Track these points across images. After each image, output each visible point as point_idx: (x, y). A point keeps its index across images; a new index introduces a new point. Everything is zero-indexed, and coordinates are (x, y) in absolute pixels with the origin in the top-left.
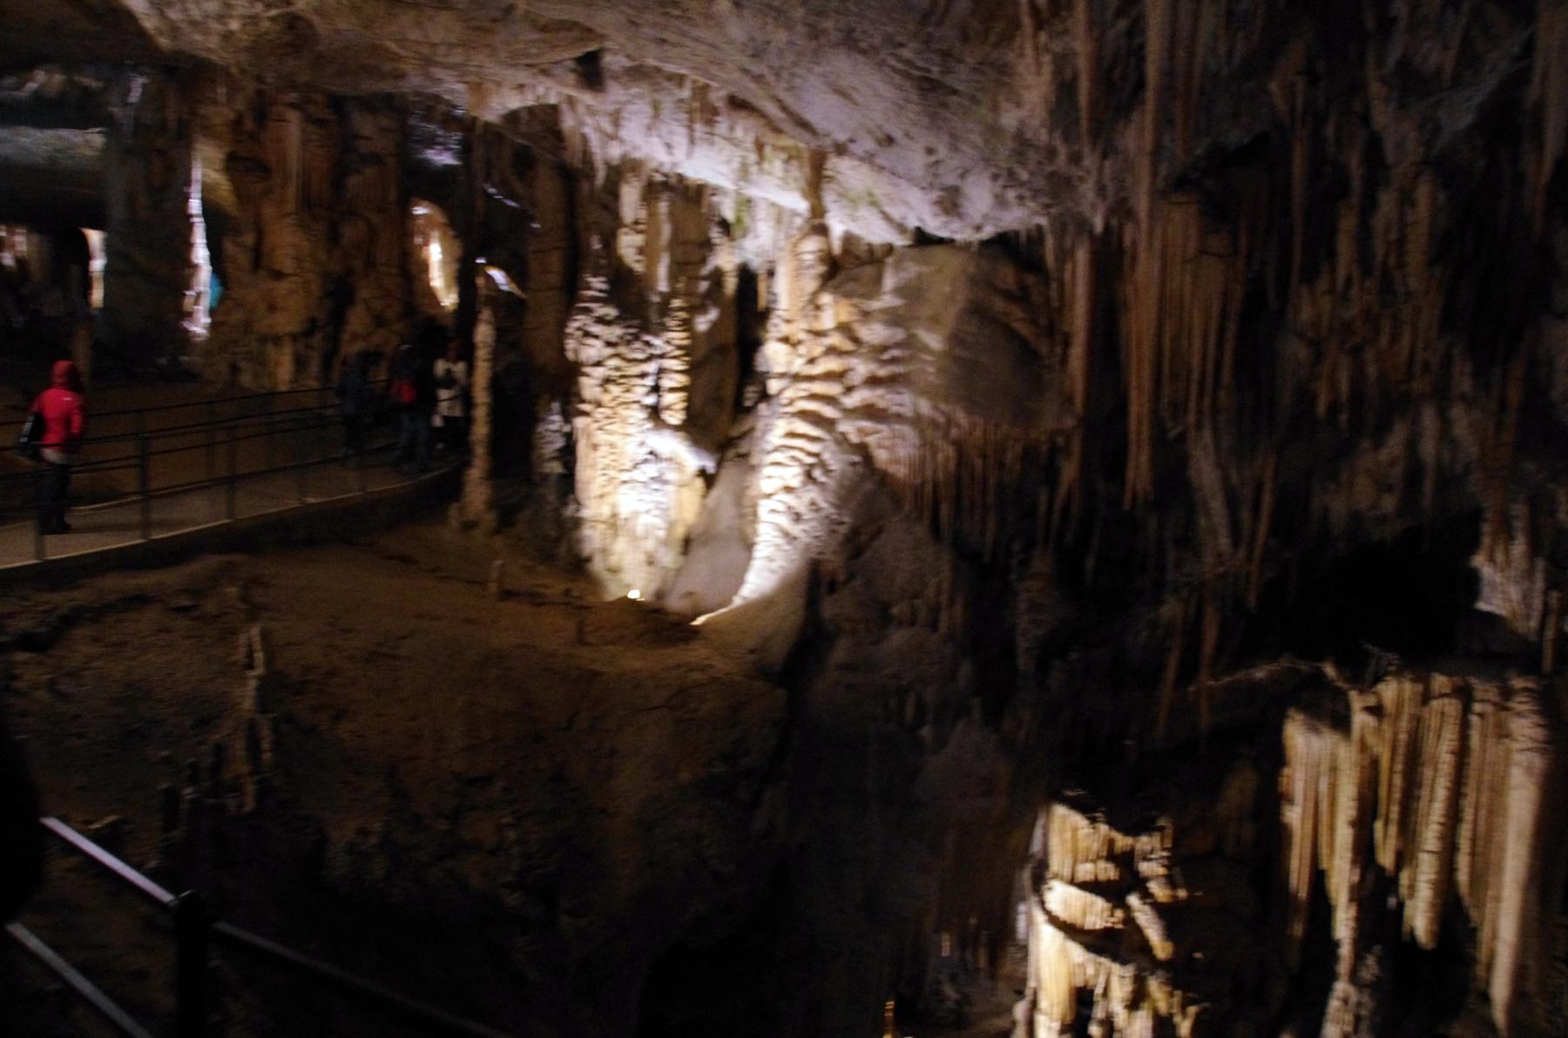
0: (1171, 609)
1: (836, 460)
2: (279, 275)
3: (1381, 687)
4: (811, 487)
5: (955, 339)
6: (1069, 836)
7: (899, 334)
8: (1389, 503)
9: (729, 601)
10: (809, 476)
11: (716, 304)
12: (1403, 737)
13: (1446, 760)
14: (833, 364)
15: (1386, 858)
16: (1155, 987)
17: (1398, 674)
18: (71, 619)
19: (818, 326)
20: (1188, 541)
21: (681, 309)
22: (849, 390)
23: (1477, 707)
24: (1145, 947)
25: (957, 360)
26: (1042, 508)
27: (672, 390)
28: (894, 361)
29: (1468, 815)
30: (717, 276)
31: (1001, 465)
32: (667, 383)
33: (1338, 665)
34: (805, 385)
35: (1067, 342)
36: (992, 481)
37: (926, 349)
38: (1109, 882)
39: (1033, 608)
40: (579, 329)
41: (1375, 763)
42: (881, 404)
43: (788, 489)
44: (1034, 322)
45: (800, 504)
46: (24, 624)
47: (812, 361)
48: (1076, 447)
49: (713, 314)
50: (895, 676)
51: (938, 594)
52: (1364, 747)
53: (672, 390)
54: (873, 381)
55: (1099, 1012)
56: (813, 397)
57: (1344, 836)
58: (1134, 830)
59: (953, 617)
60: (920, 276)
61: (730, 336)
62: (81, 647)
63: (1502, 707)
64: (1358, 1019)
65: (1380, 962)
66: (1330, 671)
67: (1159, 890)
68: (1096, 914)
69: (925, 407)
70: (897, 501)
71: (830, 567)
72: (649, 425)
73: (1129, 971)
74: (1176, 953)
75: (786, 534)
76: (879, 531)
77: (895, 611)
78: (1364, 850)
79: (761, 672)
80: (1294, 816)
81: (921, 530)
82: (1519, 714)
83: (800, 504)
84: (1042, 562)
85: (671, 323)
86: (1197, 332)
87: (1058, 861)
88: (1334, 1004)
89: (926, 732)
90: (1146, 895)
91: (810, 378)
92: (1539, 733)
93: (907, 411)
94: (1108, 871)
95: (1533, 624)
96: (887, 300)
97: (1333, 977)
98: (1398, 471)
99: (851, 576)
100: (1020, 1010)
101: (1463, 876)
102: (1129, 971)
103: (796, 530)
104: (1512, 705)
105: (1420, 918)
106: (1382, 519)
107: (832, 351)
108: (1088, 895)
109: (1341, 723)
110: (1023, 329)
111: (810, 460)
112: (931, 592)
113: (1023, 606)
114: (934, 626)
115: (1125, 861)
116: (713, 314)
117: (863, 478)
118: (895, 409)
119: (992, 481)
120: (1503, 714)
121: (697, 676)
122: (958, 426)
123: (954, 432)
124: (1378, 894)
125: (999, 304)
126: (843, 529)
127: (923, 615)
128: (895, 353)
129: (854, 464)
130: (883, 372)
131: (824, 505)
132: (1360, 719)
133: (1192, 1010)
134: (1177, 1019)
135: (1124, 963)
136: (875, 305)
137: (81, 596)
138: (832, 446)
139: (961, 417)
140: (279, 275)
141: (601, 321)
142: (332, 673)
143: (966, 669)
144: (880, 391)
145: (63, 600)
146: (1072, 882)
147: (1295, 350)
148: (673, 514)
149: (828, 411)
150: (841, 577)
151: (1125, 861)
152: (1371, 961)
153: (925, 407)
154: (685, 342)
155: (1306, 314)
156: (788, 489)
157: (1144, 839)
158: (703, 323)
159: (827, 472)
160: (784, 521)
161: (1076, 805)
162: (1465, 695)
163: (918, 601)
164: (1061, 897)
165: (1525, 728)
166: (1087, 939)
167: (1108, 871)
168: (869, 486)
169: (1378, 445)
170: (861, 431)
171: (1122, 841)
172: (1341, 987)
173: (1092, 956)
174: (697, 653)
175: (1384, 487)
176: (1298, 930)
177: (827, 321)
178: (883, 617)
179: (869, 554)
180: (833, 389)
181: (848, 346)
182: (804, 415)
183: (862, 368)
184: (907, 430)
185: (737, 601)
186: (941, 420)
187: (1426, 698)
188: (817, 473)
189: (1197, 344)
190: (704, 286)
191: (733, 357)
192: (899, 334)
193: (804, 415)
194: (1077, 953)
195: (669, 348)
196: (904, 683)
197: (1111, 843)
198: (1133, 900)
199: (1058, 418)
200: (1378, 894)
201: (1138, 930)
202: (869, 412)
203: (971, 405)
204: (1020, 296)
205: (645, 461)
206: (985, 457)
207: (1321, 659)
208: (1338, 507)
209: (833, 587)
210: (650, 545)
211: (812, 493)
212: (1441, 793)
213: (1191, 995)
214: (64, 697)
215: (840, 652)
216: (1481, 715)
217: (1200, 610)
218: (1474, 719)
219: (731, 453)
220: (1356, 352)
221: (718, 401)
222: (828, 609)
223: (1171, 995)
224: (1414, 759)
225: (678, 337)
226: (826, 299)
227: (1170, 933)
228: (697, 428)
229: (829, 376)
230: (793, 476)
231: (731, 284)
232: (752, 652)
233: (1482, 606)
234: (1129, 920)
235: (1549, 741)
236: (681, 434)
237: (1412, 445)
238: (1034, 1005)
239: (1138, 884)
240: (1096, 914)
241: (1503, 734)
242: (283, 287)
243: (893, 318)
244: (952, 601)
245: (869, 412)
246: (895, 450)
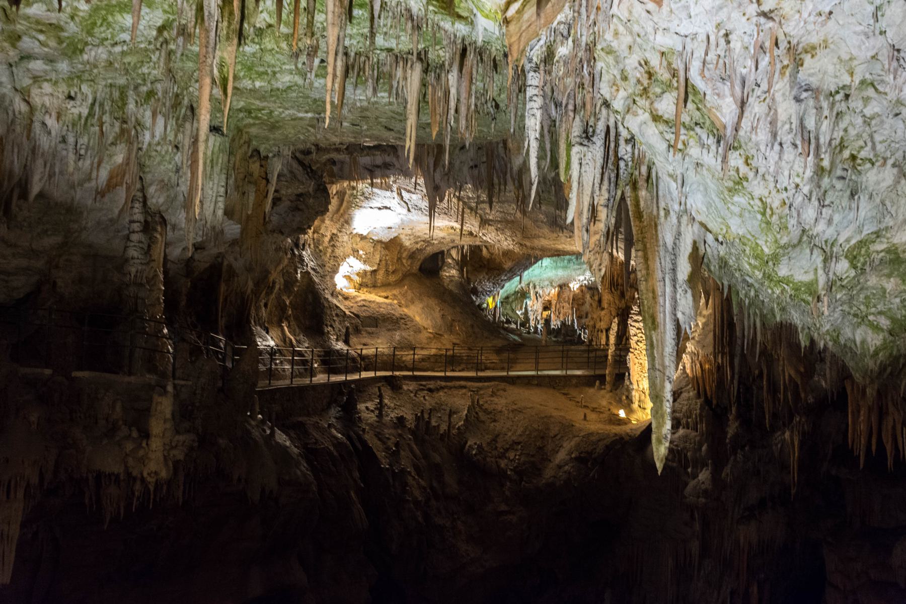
2: (603, 309)
18: (442, 388)
46: (431, 386)
62: (441, 393)
89: (689, 470)
137: (449, 384)
140: (603, 309)
141: (636, 321)
142: (501, 412)
143: (704, 448)
145: (443, 384)
214: (425, 400)
242: (603, 313)
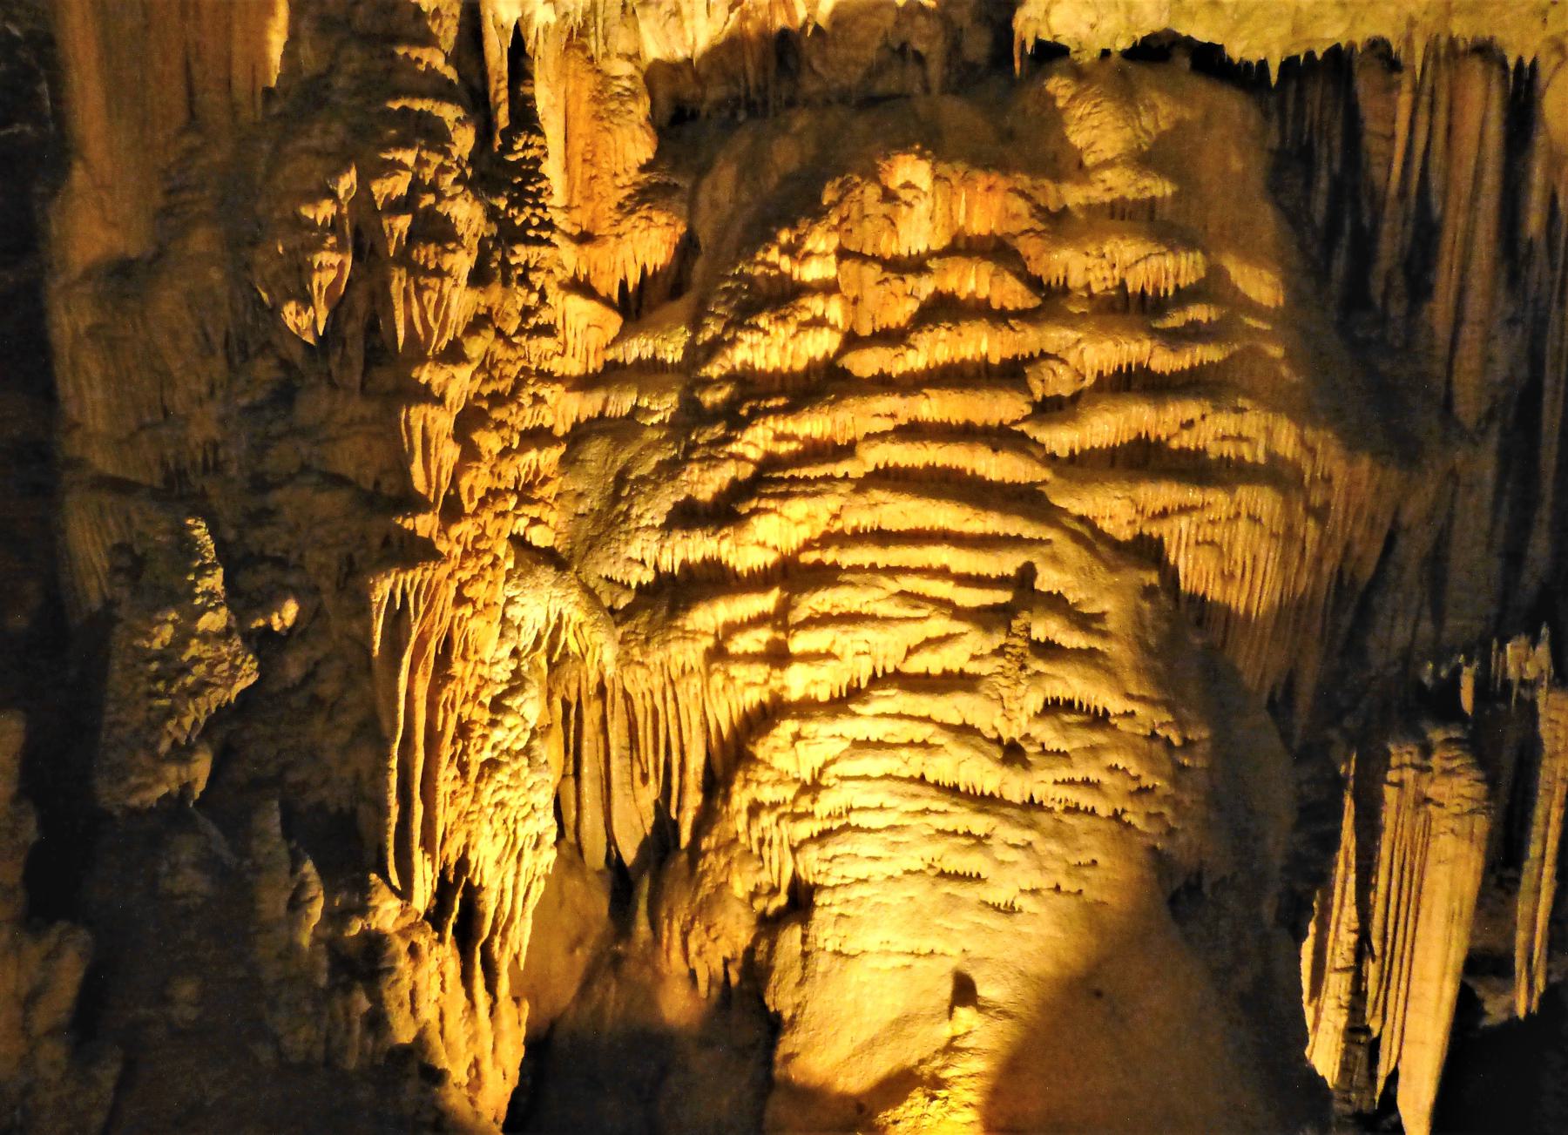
7: (1184, 267)
14: (978, 343)
40: (397, 206)
42: (1187, 440)
47: (892, 337)
54: (1129, 383)
56: (913, 431)
69: (1286, 441)
93: (1254, 454)
128: (1200, 313)
129: (1148, 592)
130: (1164, 361)
153: (1286, 441)
180: (1003, 408)
202: (1140, 459)
245: (1140, 459)
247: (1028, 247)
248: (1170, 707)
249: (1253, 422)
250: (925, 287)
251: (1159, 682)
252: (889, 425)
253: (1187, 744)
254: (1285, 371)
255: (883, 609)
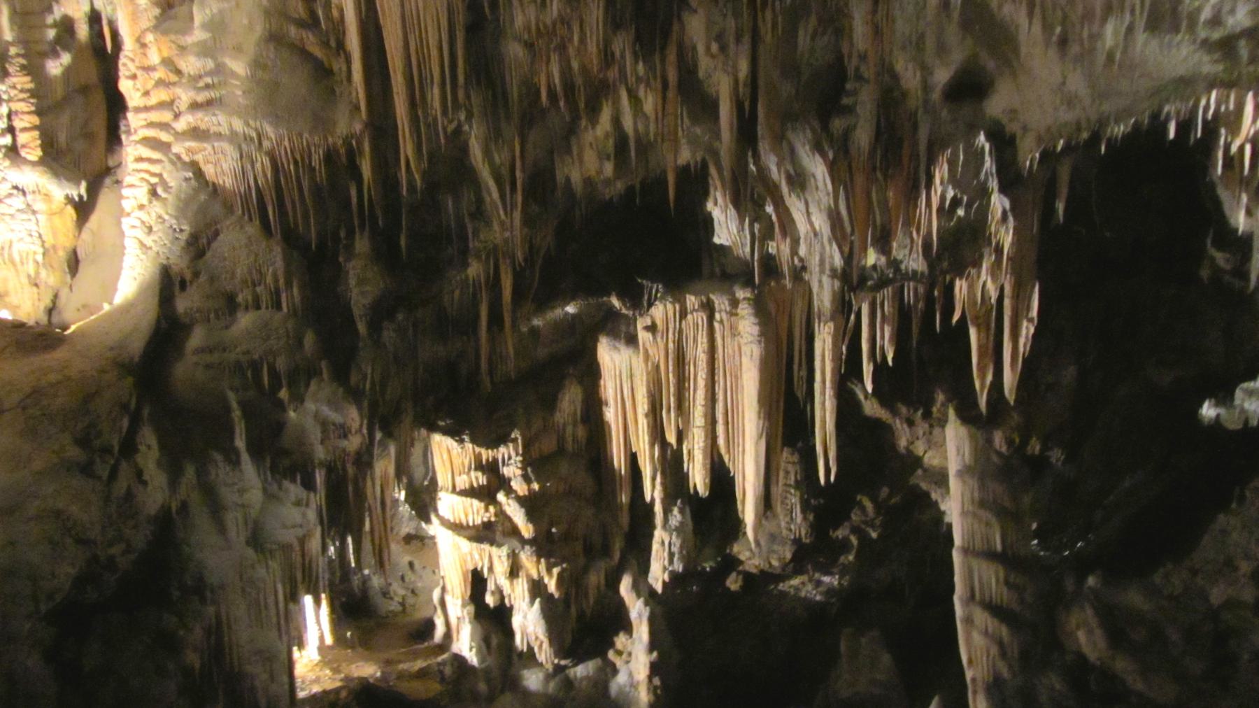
0: (474, 270)
1: (175, 179)
3: (653, 310)
4: (155, 203)
5: (257, 64)
6: (450, 457)
7: (210, 64)
8: (609, 168)
9: (101, 308)
10: (153, 193)
11: (66, 48)
12: (671, 345)
13: (702, 359)
14: (162, 95)
15: (671, 438)
16: (527, 558)
17: (663, 299)
19: (147, 63)
20: (479, 213)
21: (18, 55)
22: (177, 116)
23: (717, 316)
24: (515, 532)
25: (259, 82)
26: (354, 200)
27: (24, 130)
28: (207, 86)
29: (720, 396)
30: (67, 26)
31: (313, 169)
32: (18, 124)
33: (620, 297)
34: (143, 115)
35: (348, 62)
36: (305, 184)
37: (234, 74)
38: (481, 487)
39: (361, 283)
41: (658, 367)
42: (203, 127)
43: (141, 207)
44: (326, 44)
45: (151, 219)
48: (367, 147)
49: (66, 58)
50: (248, 352)
51: (276, 281)
52: (647, 357)
53: (24, 130)
54: (195, 106)
55: (491, 586)
56: (151, 125)
57: (643, 423)
58: (494, 444)
59: (293, 296)
60: (221, 12)
61: (91, 73)
63: (732, 314)
64: (671, 555)
65: (682, 511)
66: (616, 302)
67: (519, 486)
68: (475, 512)
69: (238, 125)
70: (229, 209)
71: (175, 269)
72: (7, 163)
73: (504, 551)
74: (536, 531)
75: (142, 245)
76: (217, 233)
77: (240, 299)
78: (657, 433)
79: (124, 367)
80: (610, 414)
81: (253, 229)
82: (743, 317)
83: (151, 219)
84: (362, 244)
85: (11, 69)
86: (433, 42)
87: (443, 478)
88: (655, 546)
89: (283, 394)
90: (509, 491)
91: (147, 109)
92: (756, 330)
93: (224, 130)
94: (480, 479)
95: (748, 249)
96: (198, 35)
97: (652, 527)
98: (611, 142)
99: (196, 275)
100: (436, 595)
101: (721, 441)
102: (504, 551)
103: (149, 241)
104: (739, 311)
105: (698, 478)
106: (608, 182)
107: (161, 83)
108: (468, 500)
109: (632, 340)
110: (318, 52)
111: (154, 180)
112: (269, 279)
113: (352, 282)
114: (278, 306)
115: (491, 469)
116: (66, 58)
117: (196, 191)
118: (213, 129)
119: (305, 184)
120: (733, 319)
121: (52, 377)
122: (269, 139)
123: (266, 144)
124: (672, 466)
125: (293, 31)
126: (184, 237)
127: (265, 299)
128: (209, 80)
129: (187, 180)
130: (201, 98)
131: (166, 217)
132: (643, 336)
133: (556, 571)
134: (546, 580)
135: (499, 546)
136: (190, 40)
138: (168, 166)
139: (269, 130)
143: (309, 339)
144: (200, 115)
146: (454, 490)
147: (514, 51)
148: (49, 240)
149: (165, 137)
150: (188, 277)
151: (491, 469)
152: (676, 511)
153: (238, 125)
154: (31, 86)
155: (519, 21)
156: (141, 207)
157: (502, 449)
158: (55, 67)
159: (167, 188)
160: (141, 234)
161: (447, 432)
162: (709, 308)
163: (258, 289)
164: (449, 505)
165: (748, 325)
166: (472, 532)
167: (480, 479)
168: (203, 197)
169: (594, 121)
170: (189, 150)
171: (487, 454)
172: (658, 534)
173: (475, 545)
174: (60, 354)
175: (603, 156)
176: (624, 498)
177: (154, 58)
178: (230, 305)
179: (209, 254)
180: (166, 116)
181: (174, 78)
182: (147, 141)
183: (185, 96)
184: (226, 146)
185: (107, 307)
186: (254, 135)
187: (683, 314)
188: (160, 191)
189: (434, 53)
190: (51, 34)
191: (99, 98)
192: (210, 64)
193: (147, 141)
194: (465, 545)
195: (13, 93)
196: (256, 357)
197: (478, 457)
198: (501, 497)
199: (349, 124)
200: (672, 466)
201: (509, 519)
202: (196, 133)
203: (276, 120)
204: (311, 22)
205: (10, 195)
206: (296, 163)
207: (609, 295)
208: (576, 177)
209: (183, 285)
210: (31, 269)
211: (157, 208)
212: (701, 383)
213: (552, 560)
215: (196, 339)
216: (721, 322)
217: (497, 268)
218: (716, 325)
219: (108, 181)
220: (562, 48)
221: (89, 136)
222: (182, 304)
223: (538, 562)
224: (681, 360)
225: (23, 81)
226: (150, 38)
227: (531, 515)
228: (56, 157)
229: (162, 105)
230: (142, 194)
231: (83, 31)
232: (112, 349)
233: (716, 240)
234: (501, 513)
235: (762, 334)
236: (41, 168)
237: (617, 121)
238: (444, 589)
239: (504, 483)
240: (475, 512)
241: (735, 333)
243: (205, 50)
244: (289, 284)
245: (196, 133)
246: (222, 166)
247: (176, 59)
248: (176, 218)
249: (222, 118)
250: (156, 75)
251: (178, 209)
252: (144, 123)
253: (181, 230)
254: (241, 100)
255: (137, 183)
